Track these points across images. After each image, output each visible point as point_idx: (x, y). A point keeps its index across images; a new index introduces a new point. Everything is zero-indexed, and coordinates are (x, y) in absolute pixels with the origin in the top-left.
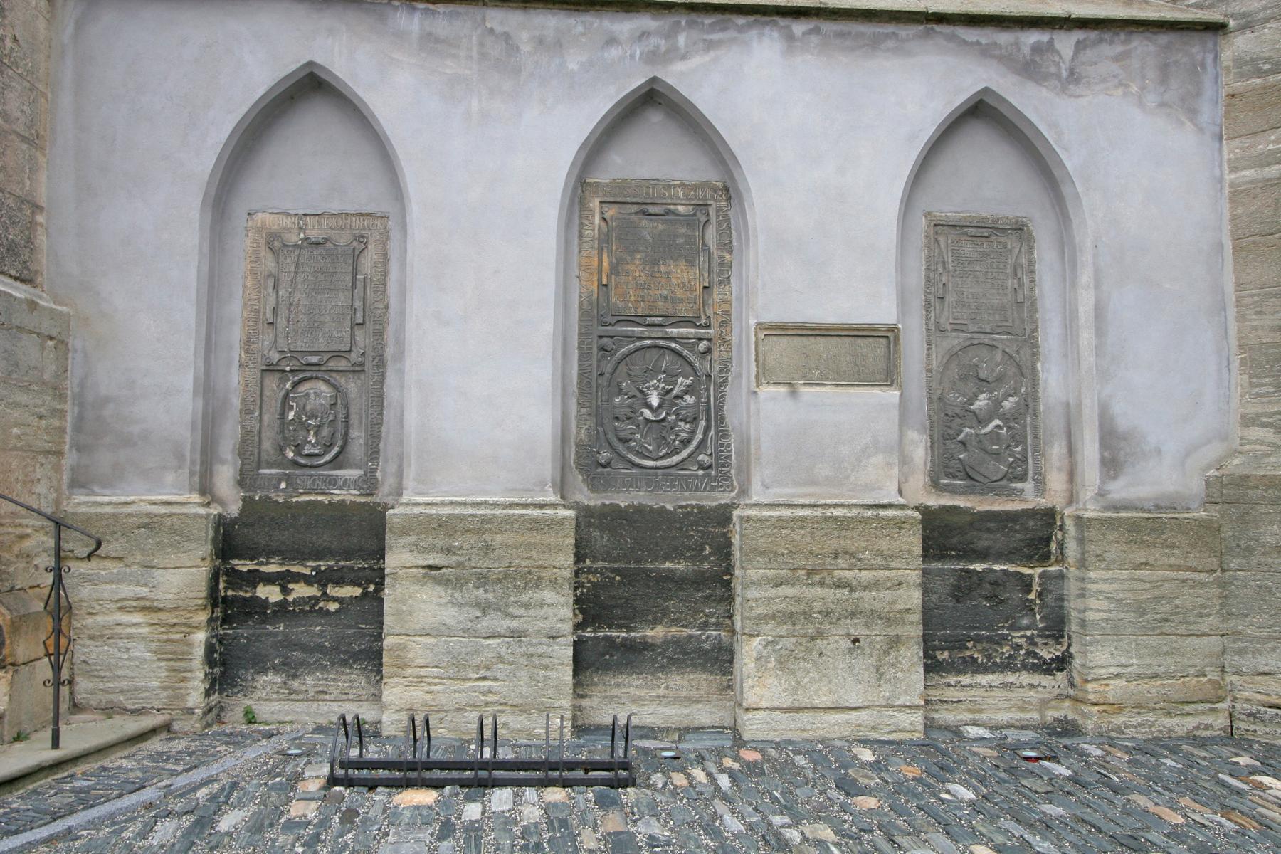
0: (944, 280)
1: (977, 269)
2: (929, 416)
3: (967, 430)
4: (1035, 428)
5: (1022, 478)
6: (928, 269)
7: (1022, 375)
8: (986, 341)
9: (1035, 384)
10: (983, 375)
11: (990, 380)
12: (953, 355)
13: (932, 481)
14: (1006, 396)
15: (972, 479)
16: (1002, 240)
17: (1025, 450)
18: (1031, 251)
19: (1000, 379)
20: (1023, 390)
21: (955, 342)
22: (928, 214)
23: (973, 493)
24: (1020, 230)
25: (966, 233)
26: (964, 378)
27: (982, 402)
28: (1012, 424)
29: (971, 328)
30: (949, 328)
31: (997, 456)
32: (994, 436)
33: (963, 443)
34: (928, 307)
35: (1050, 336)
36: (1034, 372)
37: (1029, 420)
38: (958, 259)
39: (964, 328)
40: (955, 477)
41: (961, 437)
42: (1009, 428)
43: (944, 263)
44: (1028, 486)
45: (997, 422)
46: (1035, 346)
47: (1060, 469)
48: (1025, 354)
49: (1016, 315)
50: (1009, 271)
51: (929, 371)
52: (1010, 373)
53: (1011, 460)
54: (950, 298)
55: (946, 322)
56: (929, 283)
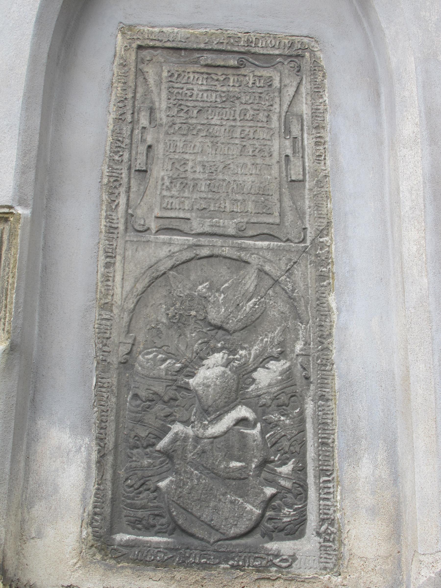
0: (149, 139)
1: (216, 120)
2: (99, 396)
3: (177, 428)
4: (324, 425)
5: (295, 530)
6: (120, 119)
7: (298, 317)
8: (226, 252)
9: (323, 337)
10: (215, 315)
11: (231, 325)
12: (157, 278)
13: (97, 536)
14: (263, 360)
15: (184, 531)
16: (265, 73)
17: (301, 470)
18: (317, 91)
19: (251, 326)
20: (299, 347)
21: (163, 252)
22: (126, 29)
23: (184, 564)
24: (297, 57)
25: (196, 62)
26: (179, 322)
27: (211, 372)
28: (274, 417)
29: (197, 226)
30: (153, 227)
31: (238, 482)
32: (233, 443)
33: (168, 455)
34: (112, 186)
35: (354, 246)
36: (323, 312)
37: (310, 407)
38: (179, 104)
39: (184, 227)
40: (149, 529)
41: (162, 444)
42: (268, 425)
43: (152, 110)
44: (307, 546)
45: (243, 412)
46: (323, 261)
47: (373, 511)
48: (304, 276)
49: (287, 203)
50: (275, 124)
51: (106, 307)
52: (273, 313)
53: (269, 491)
54: (160, 172)
55: (149, 211)
56: (117, 146)
